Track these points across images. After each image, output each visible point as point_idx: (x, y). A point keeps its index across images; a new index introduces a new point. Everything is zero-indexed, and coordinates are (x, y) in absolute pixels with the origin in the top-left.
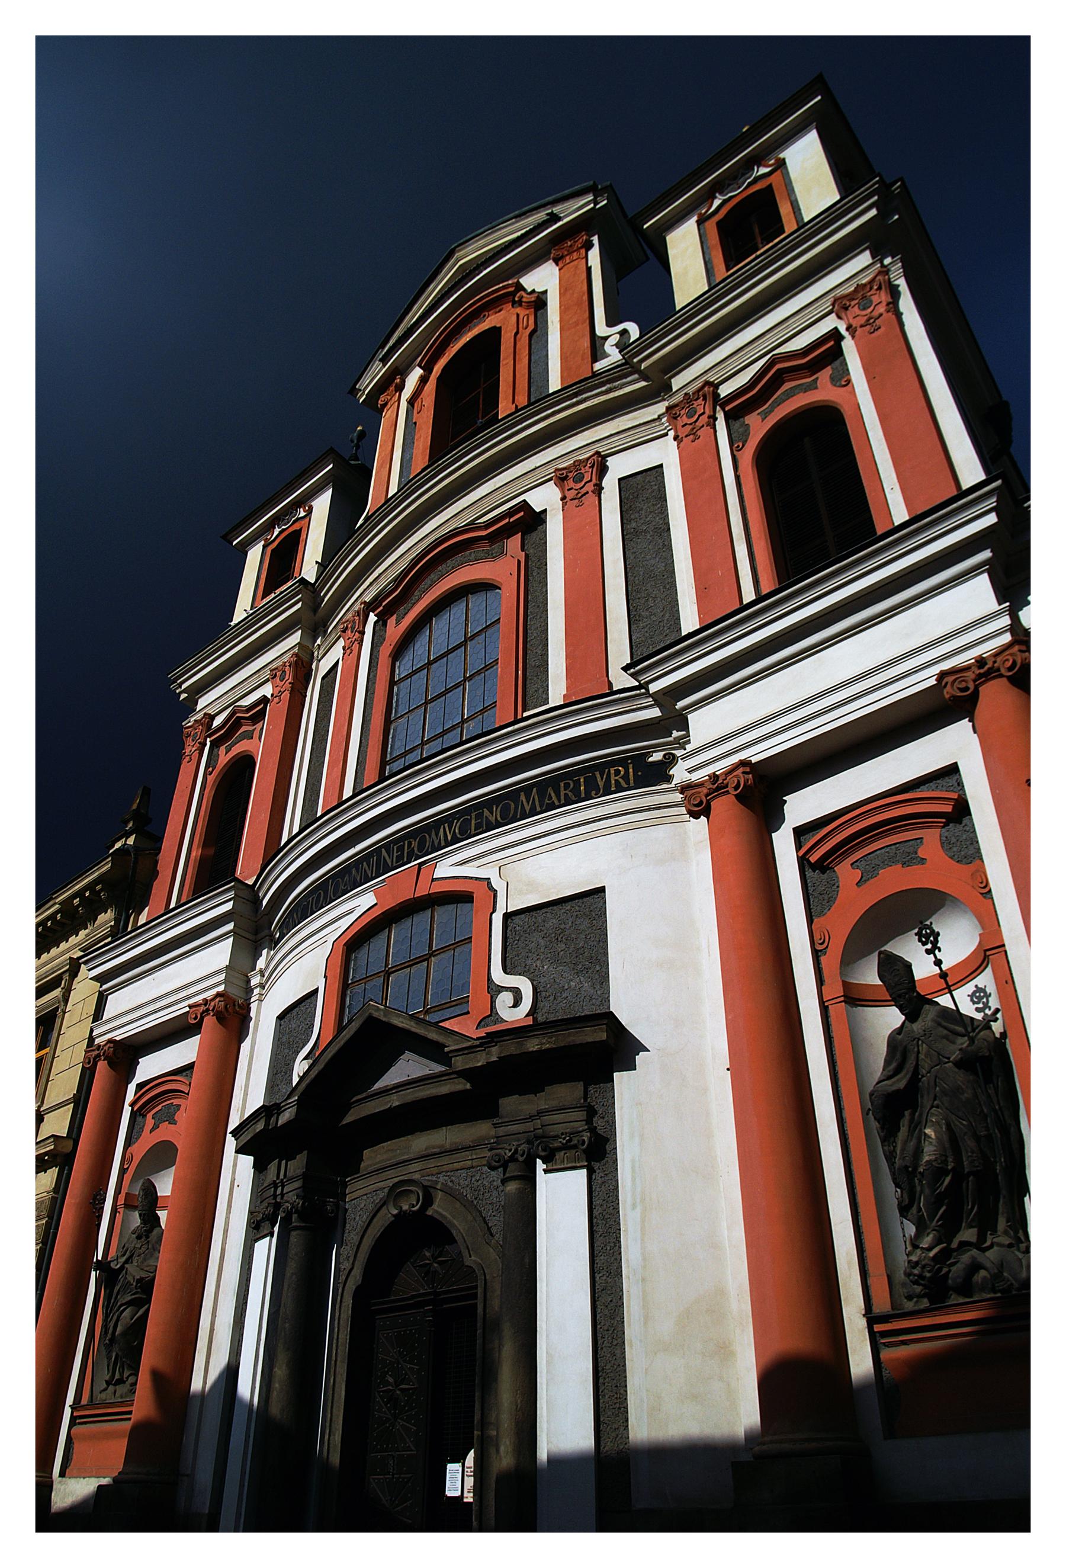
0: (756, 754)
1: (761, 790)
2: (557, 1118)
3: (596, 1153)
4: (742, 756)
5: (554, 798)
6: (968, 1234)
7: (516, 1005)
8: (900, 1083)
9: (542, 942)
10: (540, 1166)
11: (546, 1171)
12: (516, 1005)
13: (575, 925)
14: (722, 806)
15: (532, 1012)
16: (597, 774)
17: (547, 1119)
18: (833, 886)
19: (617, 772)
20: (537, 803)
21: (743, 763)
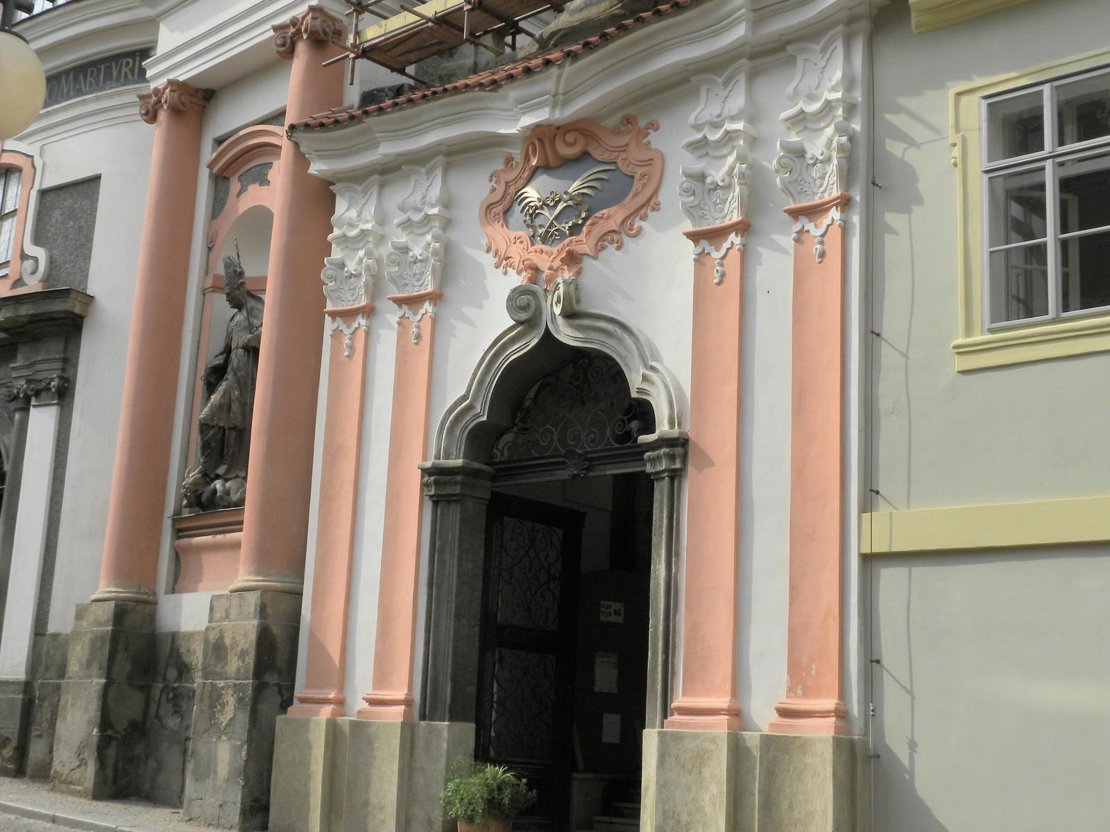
0: (182, 75)
1: (196, 101)
2: (44, 366)
3: (64, 394)
4: (171, 76)
5: (83, 86)
6: (221, 470)
7: (33, 273)
8: (220, 361)
9: (60, 218)
10: (33, 402)
11: (34, 406)
12: (33, 273)
13: (68, 209)
14: (163, 116)
15: (46, 280)
16: (114, 63)
17: (38, 367)
18: (227, 193)
19: (128, 63)
20: (72, 88)
21: (171, 82)
